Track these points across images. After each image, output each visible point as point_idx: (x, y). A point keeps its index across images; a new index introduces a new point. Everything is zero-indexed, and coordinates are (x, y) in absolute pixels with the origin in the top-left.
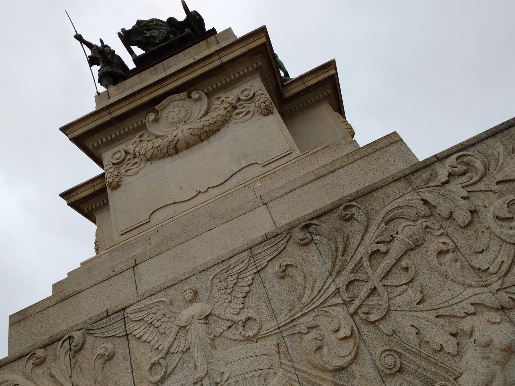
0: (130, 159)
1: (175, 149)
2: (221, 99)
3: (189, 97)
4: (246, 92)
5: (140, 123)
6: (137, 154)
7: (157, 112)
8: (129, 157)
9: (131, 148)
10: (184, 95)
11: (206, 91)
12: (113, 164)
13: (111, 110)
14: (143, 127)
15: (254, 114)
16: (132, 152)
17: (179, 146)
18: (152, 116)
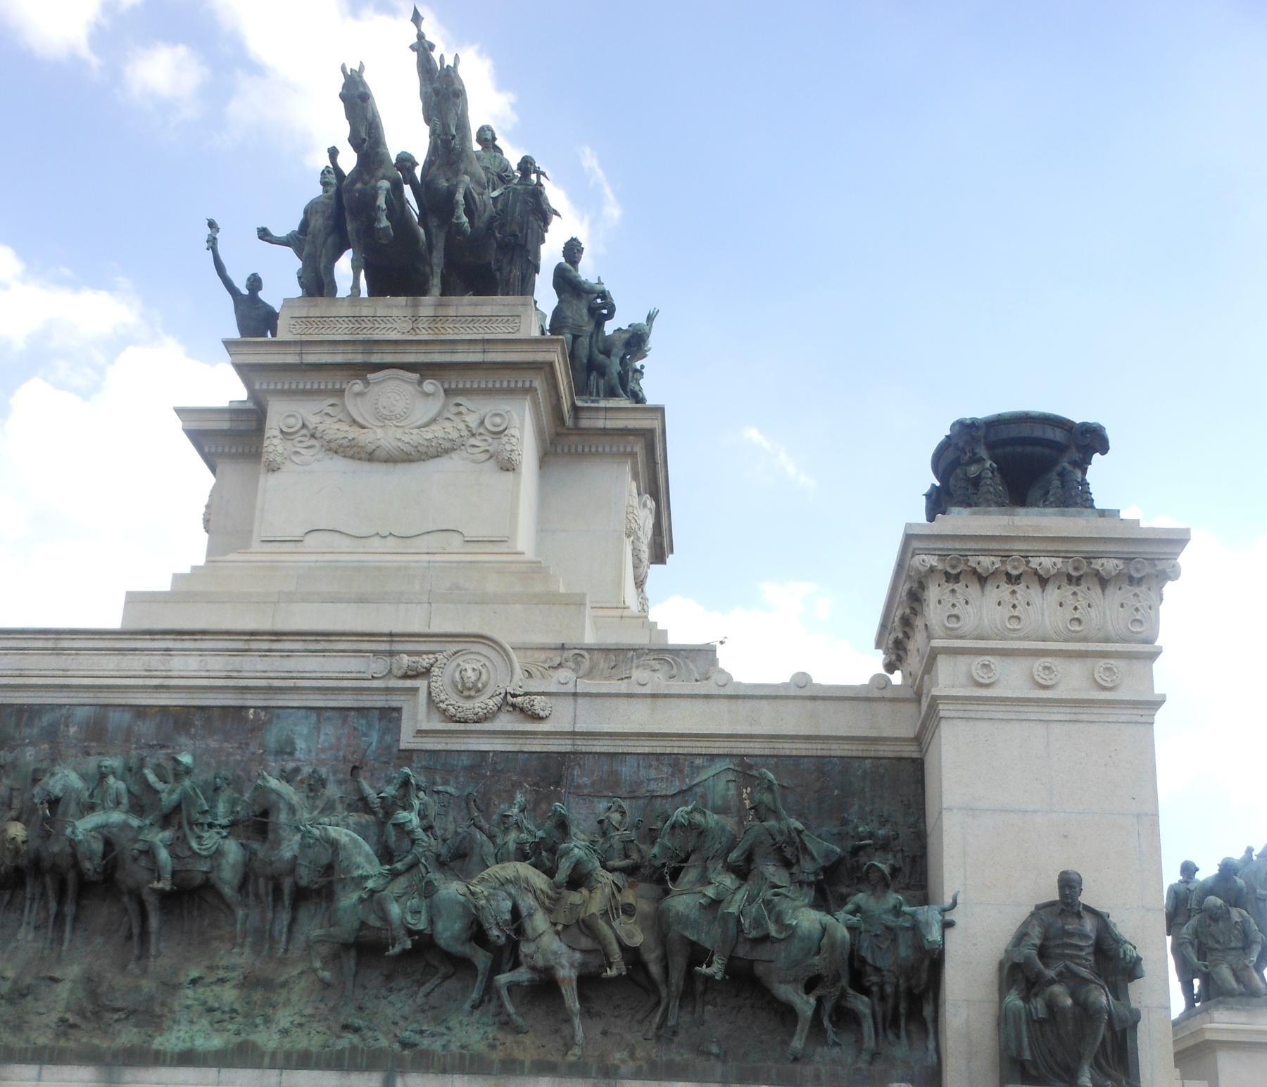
0: (305, 436)
1: (370, 456)
2: (462, 409)
3: (420, 383)
4: (498, 420)
5: (337, 386)
6: (318, 435)
7: (367, 383)
8: (304, 431)
9: (313, 421)
10: (416, 376)
11: (446, 386)
12: (282, 432)
13: (305, 349)
14: (342, 391)
15: (491, 457)
16: (311, 427)
17: (377, 453)
18: (358, 386)
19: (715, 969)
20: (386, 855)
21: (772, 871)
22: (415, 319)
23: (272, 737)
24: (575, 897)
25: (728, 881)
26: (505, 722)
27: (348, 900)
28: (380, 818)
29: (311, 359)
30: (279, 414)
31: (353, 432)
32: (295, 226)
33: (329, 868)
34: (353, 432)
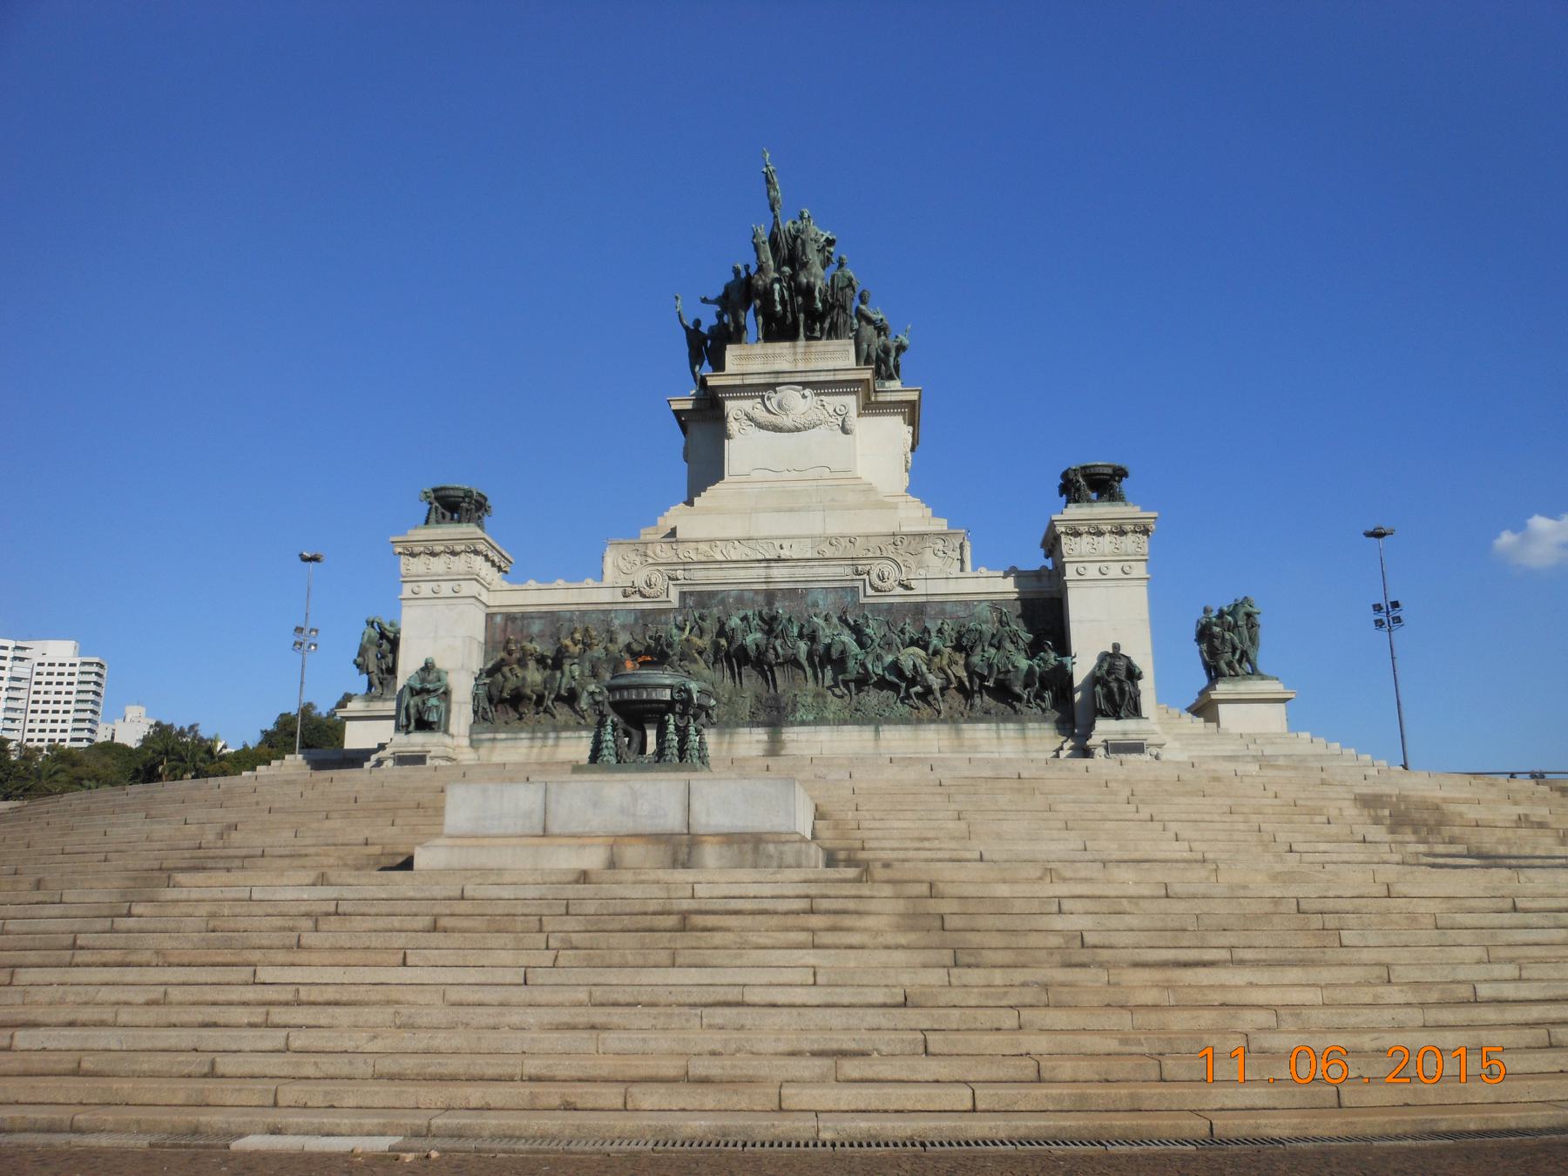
9: (750, 411)
18: (772, 394)
19: (991, 683)
20: (862, 645)
21: (1009, 646)
22: (795, 354)
23: (810, 600)
24: (937, 659)
25: (993, 651)
26: (900, 591)
27: (851, 664)
28: (857, 631)
29: (748, 381)
30: (732, 407)
31: (771, 418)
32: (720, 291)
33: (843, 652)
34: (771, 418)
